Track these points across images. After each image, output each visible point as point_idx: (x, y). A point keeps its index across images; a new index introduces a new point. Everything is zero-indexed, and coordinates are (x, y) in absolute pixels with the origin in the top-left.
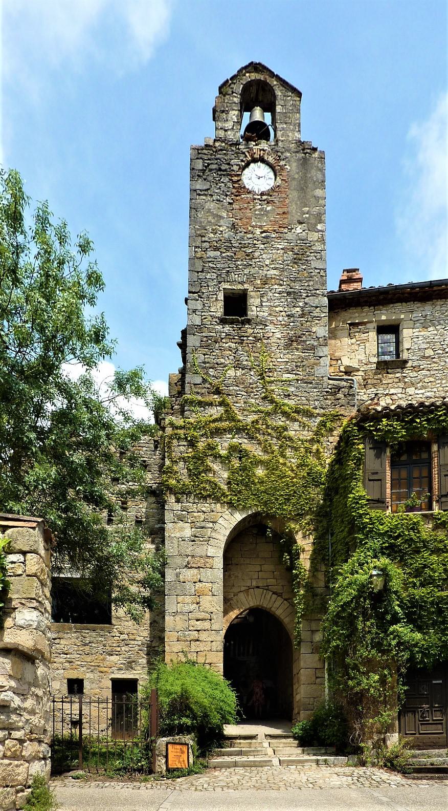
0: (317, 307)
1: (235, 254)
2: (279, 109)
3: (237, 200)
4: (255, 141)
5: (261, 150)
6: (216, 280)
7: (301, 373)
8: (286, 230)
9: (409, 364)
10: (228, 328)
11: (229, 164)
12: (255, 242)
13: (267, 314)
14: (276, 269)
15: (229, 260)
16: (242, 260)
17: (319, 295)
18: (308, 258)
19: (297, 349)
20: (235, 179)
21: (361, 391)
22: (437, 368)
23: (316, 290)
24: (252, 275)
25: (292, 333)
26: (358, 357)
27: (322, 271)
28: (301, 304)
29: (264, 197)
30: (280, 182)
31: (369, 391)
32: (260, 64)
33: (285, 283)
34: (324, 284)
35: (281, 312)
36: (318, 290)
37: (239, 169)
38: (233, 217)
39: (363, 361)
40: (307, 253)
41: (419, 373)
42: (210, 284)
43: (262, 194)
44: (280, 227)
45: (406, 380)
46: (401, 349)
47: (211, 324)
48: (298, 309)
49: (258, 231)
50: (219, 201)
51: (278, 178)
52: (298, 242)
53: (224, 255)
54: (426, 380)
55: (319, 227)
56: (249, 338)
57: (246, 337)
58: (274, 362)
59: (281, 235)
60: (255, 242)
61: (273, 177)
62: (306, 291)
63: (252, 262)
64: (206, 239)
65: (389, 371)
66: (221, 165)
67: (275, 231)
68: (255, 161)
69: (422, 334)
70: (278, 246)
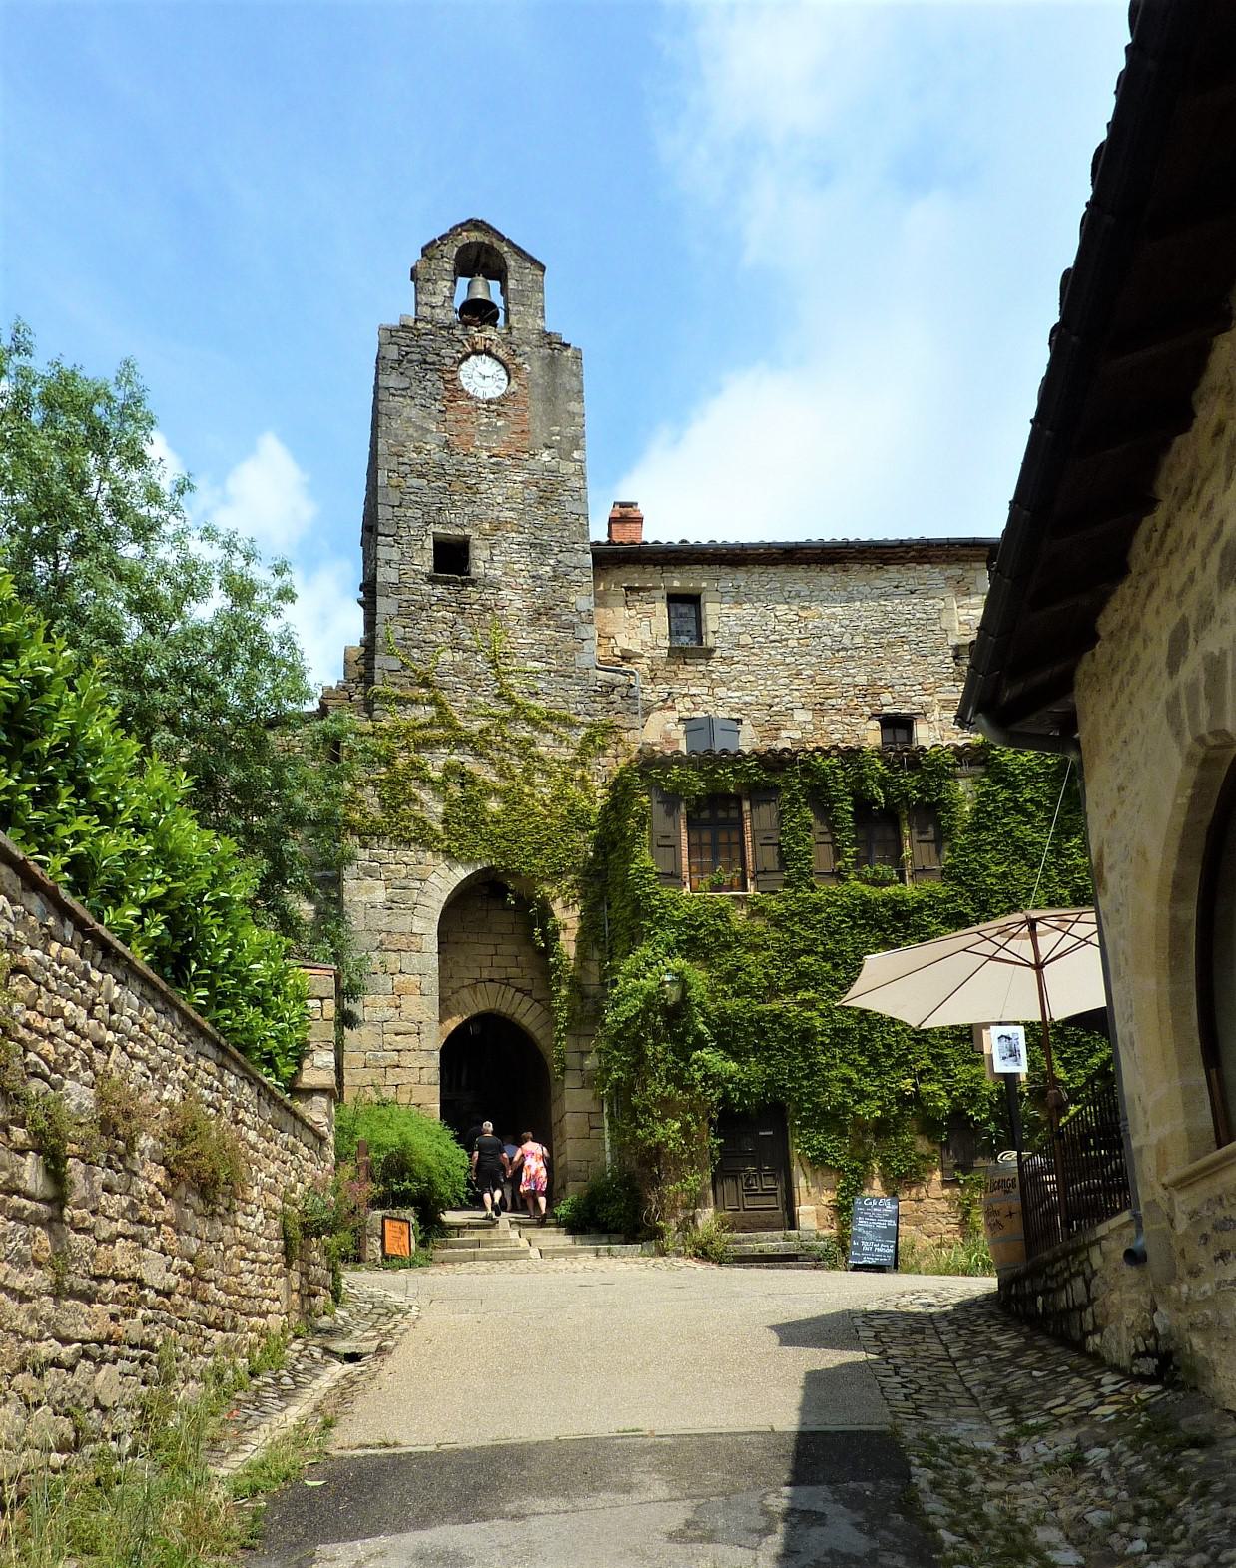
0: (575, 568)
2: (512, 285)
8: (526, 456)
9: (717, 653)
11: (438, 355)
12: (480, 469)
14: (513, 510)
19: (548, 626)
28: (552, 562)
29: (493, 407)
32: (482, 221)
34: (586, 534)
43: (489, 402)
48: (548, 568)
49: (485, 455)
53: (433, 485)
55: (576, 455)
60: (480, 469)
61: (506, 379)
64: (406, 460)
67: (510, 456)
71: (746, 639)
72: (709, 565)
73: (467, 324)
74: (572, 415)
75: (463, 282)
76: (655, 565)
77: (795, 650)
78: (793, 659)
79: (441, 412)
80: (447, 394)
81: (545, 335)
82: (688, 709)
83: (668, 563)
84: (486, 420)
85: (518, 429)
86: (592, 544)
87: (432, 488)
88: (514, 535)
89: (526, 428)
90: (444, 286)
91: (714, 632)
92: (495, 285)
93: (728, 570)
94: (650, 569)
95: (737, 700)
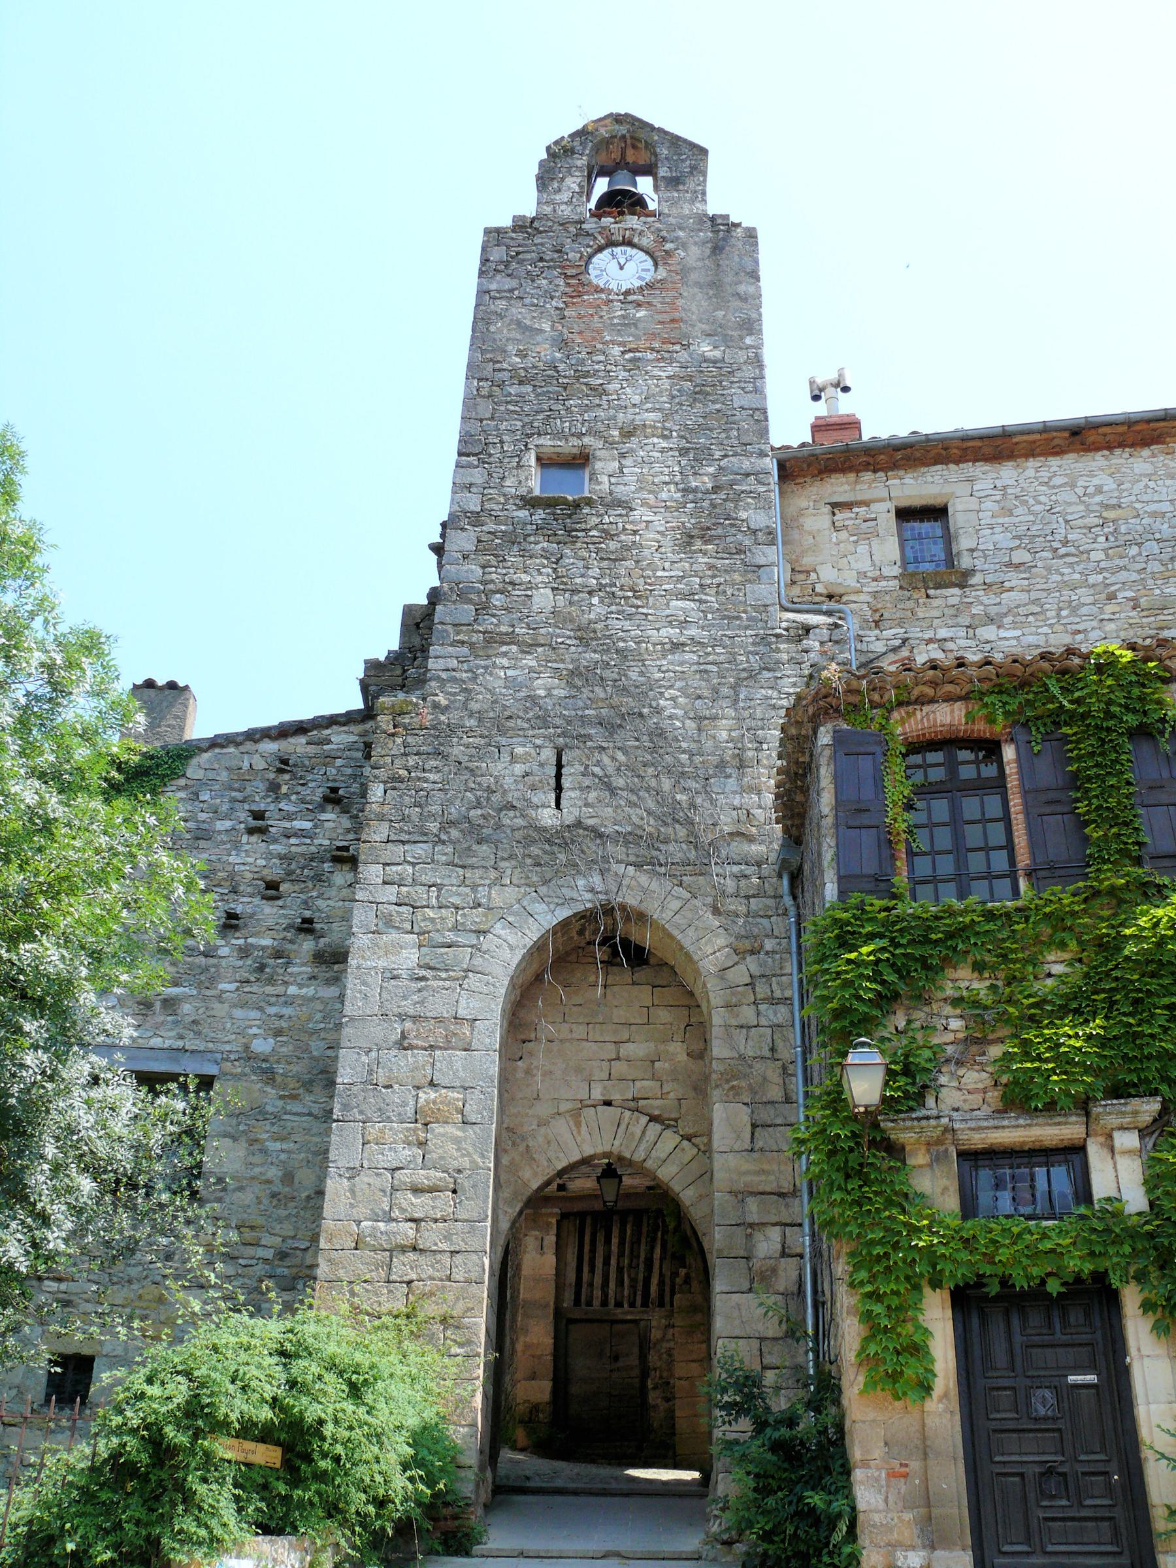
0: (748, 475)
3: (574, 304)
4: (614, 217)
6: (519, 433)
7: (713, 599)
8: (678, 347)
9: (976, 579)
10: (543, 516)
12: (609, 367)
13: (633, 488)
14: (653, 410)
16: (579, 398)
17: (752, 453)
20: (570, 272)
21: (868, 632)
22: (1044, 586)
23: (746, 445)
25: (693, 521)
29: (631, 298)
31: (888, 633)
32: (627, 115)
34: (764, 433)
39: (869, 574)
41: (1003, 596)
42: (506, 438)
43: (627, 293)
44: (663, 343)
45: (974, 611)
46: (954, 551)
49: (616, 351)
51: (660, 268)
52: (705, 365)
54: (1021, 610)
56: (591, 534)
57: (583, 530)
58: (649, 577)
60: (609, 367)
64: (505, 366)
65: (931, 592)
67: (652, 349)
69: (1000, 520)
71: (1020, 556)
72: (957, 463)
74: (744, 299)
76: (875, 471)
77: (1103, 564)
78: (1100, 578)
79: (557, 308)
80: (568, 290)
83: (895, 466)
84: (619, 313)
85: (667, 317)
87: (538, 395)
88: (656, 440)
89: (677, 315)
90: (573, 183)
91: (972, 550)
93: (986, 467)
94: (868, 476)
95: (1014, 642)
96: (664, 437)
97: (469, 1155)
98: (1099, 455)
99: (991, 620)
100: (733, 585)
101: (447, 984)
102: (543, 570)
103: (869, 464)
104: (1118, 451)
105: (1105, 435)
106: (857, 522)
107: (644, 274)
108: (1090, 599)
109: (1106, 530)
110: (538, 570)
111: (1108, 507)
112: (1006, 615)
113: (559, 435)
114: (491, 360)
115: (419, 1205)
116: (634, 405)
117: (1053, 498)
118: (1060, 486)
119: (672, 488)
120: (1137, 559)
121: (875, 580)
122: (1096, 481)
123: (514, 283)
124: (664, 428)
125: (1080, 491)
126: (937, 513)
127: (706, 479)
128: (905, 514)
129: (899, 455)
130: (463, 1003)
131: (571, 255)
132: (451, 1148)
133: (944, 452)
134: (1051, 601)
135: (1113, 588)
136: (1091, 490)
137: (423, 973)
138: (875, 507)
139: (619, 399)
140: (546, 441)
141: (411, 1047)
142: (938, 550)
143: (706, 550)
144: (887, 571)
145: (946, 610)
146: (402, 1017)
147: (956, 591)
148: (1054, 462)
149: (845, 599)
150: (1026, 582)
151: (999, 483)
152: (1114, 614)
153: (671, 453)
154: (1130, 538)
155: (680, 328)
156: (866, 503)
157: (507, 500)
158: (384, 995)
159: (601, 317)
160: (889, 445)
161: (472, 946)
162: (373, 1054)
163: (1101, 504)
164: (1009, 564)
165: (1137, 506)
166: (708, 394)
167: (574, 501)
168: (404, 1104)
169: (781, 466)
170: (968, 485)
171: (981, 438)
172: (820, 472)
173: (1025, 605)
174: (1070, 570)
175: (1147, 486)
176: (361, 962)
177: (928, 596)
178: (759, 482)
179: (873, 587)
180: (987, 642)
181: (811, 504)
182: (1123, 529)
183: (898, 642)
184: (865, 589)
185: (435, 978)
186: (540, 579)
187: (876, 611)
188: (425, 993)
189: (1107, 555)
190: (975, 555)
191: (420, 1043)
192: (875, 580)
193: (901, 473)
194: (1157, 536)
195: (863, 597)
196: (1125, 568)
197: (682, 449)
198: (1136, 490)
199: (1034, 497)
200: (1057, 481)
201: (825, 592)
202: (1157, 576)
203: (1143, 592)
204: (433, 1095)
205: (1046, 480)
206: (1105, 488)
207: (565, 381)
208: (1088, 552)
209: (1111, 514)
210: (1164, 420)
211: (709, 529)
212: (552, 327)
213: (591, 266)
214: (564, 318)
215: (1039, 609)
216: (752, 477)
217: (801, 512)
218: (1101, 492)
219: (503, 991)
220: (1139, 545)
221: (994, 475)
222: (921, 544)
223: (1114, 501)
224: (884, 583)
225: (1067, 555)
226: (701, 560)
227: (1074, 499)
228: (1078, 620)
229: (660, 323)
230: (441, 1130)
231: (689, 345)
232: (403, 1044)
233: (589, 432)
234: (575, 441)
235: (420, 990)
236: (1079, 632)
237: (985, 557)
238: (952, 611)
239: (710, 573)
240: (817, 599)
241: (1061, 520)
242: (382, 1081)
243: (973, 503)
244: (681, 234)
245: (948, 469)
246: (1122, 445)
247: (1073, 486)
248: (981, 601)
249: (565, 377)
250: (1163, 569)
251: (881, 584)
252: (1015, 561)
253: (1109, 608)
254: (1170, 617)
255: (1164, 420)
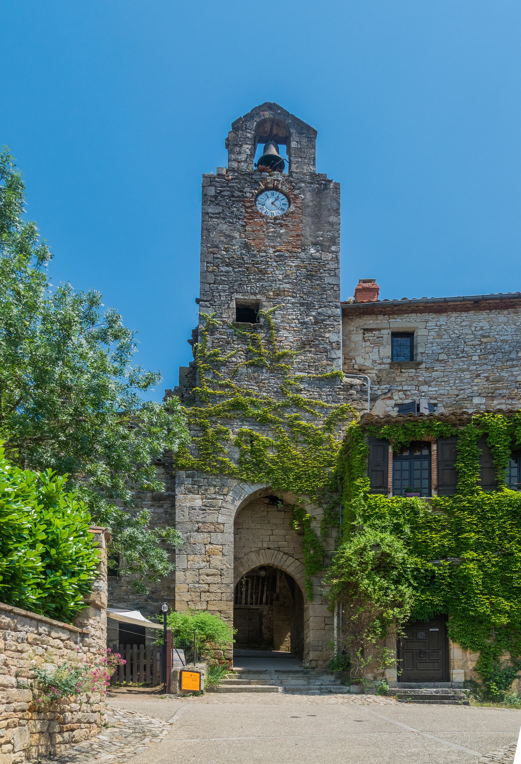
0: (329, 317)
1: (248, 270)
2: (293, 144)
3: (250, 223)
4: (269, 172)
5: (275, 180)
6: (227, 291)
7: (314, 372)
8: (300, 250)
9: (423, 366)
11: (242, 192)
12: (268, 259)
13: (280, 321)
14: (288, 283)
15: (241, 274)
16: (254, 275)
17: (332, 306)
18: (321, 275)
19: (310, 352)
20: (248, 204)
21: (375, 386)
22: (451, 370)
23: (329, 302)
24: (265, 287)
26: (371, 357)
27: (336, 287)
28: (314, 313)
29: (278, 221)
30: (294, 209)
31: (383, 387)
32: (274, 104)
33: (298, 295)
34: (337, 297)
35: (294, 319)
36: (331, 302)
37: (252, 196)
38: (245, 238)
39: (377, 361)
40: (321, 271)
41: (433, 373)
42: (222, 294)
43: (276, 219)
44: (293, 248)
45: (420, 379)
46: (415, 353)
47: (223, 328)
48: (311, 318)
49: (271, 251)
50: (232, 223)
51: (292, 205)
52: (312, 260)
53: (236, 270)
54: (439, 380)
55: (333, 248)
59: (294, 254)
60: (268, 259)
61: (287, 203)
62: (319, 303)
63: (265, 276)
64: (219, 256)
65: (403, 370)
66: (234, 192)
67: (288, 250)
68: (267, 189)
69: (437, 341)
70: (291, 264)
71: (443, 357)
72: (421, 313)
73: (262, 171)
74: (332, 224)
75: (260, 147)
76: (384, 315)
77: (477, 362)
78: (475, 367)
79: (242, 225)
81: (313, 175)
82: (401, 399)
83: (393, 313)
84: (272, 230)
85: (294, 233)
86: (342, 303)
87: (235, 272)
88: (289, 298)
89: (300, 233)
90: (247, 148)
91: (422, 353)
92: (283, 148)
93: (434, 316)
94: (381, 317)
95: (435, 393)
96: (293, 297)
97: (225, 565)
98: (484, 313)
99: (426, 383)
100: (322, 366)
101: (214, 512)
102: (241, 357)
103: (382, 311)
104: (493, 311)
105: (489, 303)
106: (374, 338)
107: (283, 207)
108: (469, 376)
109: (481, 347)
110: (239, 357)
111: (484, 337)
112: (433, 381)
113: (244, 293)
114: (212, 252)
115: (210, 579)
116: (280, 280)
117: (461, 331)
118: (465, 326)
119: (297, 321)
120: (492, 360)
121: (380, 364)
122: (481, 324)
123: (220, 209)
124: (294, 293)
125: (473, 329)
126: (410, 335)
127: (311, 318)
128: (395, 335)
129: (396, 308)
130: (220, 518)
131: (248, 195)
132: (219, 563)
133: (416, 308)
134: (452, 376)
135: (479, 372)
136: (478, 328)
137: (204, 508)
138: (383, 332)
139: (272, 277)
140: (239, 296)
141: (202, 532)
142: (407, 352)
143: (311, 351)
144: (385, 361)
145: (408, 378)
146: (198, 522)
147: (413, 370)
148: (464, 314)
149: (366, 372)
150: (443, 368)
151: (438, 324)
152: (477, 383)
153: (296, 305)
154: (491, 351)
155: (301, 240)
156: (379, 330)
157: (224, 324)
158: (190, 515)
159: (264, 232)
160: (392, 304)
161: (222, 499)
162: (188, 534)
163: (481, 335)
164: (438, 360)
165: (496, 336)
166: (313, 276)
167: (254, 326)
168: (201, 549)
169: (343, 311)
170: (424, 323)
171: (434, 303)
172: (360, 314)
173: (442, 377)
174: (463, 364)
175: (503, 328)
176: (181, 504)
177: (401, 372)
178: (335, 320)
179: (379, 367)
180: (424, 392)
181: (355, 329)
182: (488, 347)
183: (386, 391)
184: (375, 368)
185: (209, 510)
186: (240, 361)
187: (379, 377)
188: (205, 515)
189: (479, 358)
190: (423, 355)
191: (205, 530)
192: (380, 364)
193: (396, 316)
194: (503, 351)
195: (374, 371)
196: (486, 364)
197: (301, 303)
198: (498, 330)
199: (453, 331)
200: (464, 324)
201: (358, 368)
202: (499, 368)
203: (492, 374)
204: (211, 546)
205: (459, 323)
206: (485, 328)
207: (248, 266)
208: (472, 356)
209: (484, 340)
210: (517, 298)
211: (312, 341)
212: (240, 236)
213: (257, 202)
214: (246, 231)
215: (447, 380)
216: (332, 318)
217: (350, 332)
218: (482, 330)
219: (234, 514)
220: (494, 354)
221: (437, 319)
222: (400, 348)
223: (487, 334)
224: (383, 366)
225: (463, 357)
226: (308, 355)
227: (470, 332)
228: (462, 385)
229: (293, 237)
230: (215, 557)
231: (305, 249)
232: (198, 530)
233: (259, 293)
234: (252, 297)
235: (203, 514)
236: (462, 390)
237: (428, 356)
238: (411, 379)
239: (312, 361)
240: (355, 371)
241: (462, 341)
242: (192, 542)
243: (426, 332)
244: (303, 185)
245: (417, 316)
246: (496, 308)
247: (470, 326)
248: (423, 375)
249: (247, 264)
250: (502, 365)
251: (382, 366)
252: (440, 358)
253: (476, 381)
254: (501, 385)
255: (517, 298)
